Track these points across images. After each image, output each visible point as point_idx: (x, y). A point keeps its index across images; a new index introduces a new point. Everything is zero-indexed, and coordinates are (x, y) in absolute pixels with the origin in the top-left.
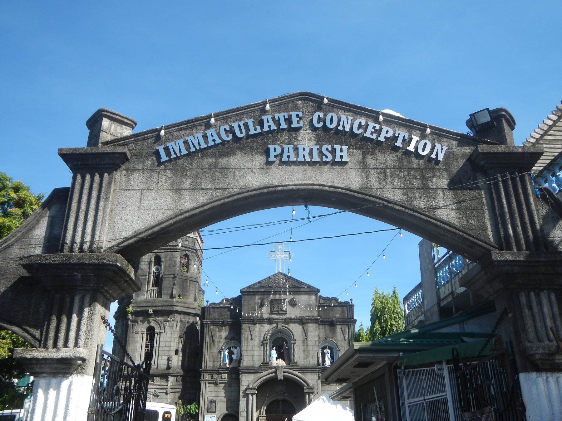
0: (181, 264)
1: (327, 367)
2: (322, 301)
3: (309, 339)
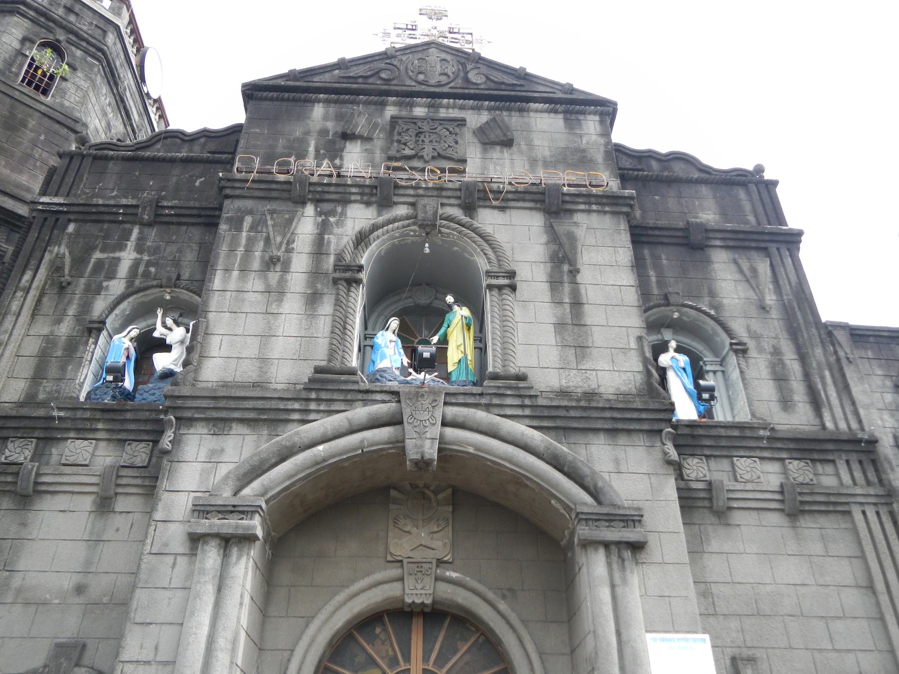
0: (20, 58)
1: (691, 425)
2: (627, 163)
3: (585, 277)
